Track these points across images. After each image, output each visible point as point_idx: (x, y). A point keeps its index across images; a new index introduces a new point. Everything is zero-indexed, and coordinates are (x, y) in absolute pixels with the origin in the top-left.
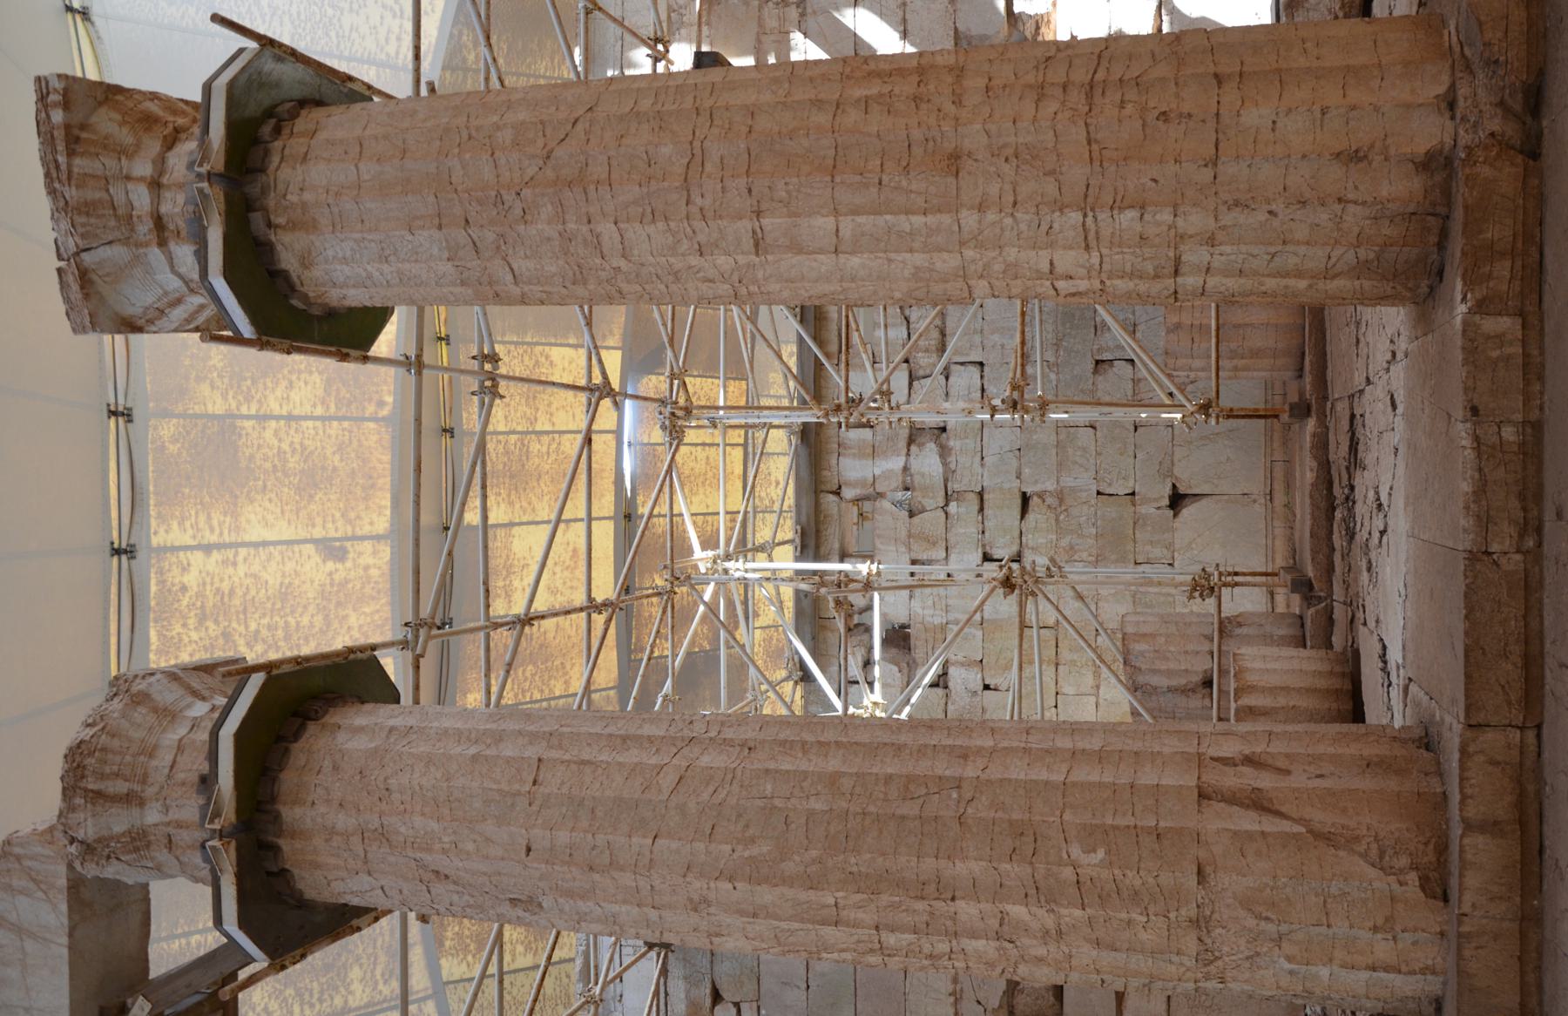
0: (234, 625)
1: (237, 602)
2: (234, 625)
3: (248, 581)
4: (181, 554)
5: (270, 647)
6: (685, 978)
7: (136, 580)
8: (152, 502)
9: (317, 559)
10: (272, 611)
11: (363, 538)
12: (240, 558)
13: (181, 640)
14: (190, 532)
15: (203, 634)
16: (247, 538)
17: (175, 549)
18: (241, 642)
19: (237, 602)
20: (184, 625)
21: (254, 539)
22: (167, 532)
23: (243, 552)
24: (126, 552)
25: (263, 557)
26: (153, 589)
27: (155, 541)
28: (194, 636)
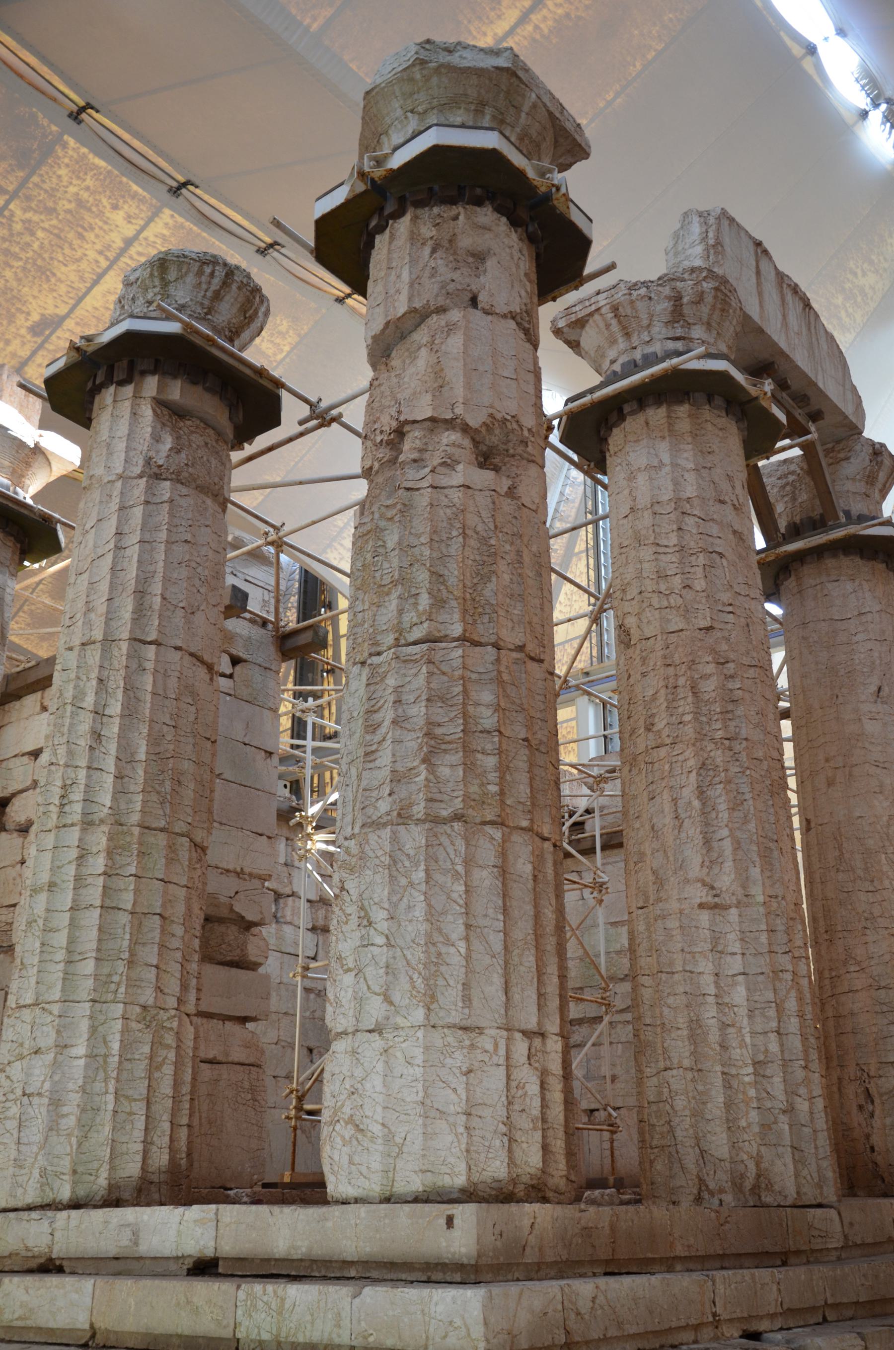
0: (54, 222)
1: (71, 235)
2: (54, 222)
3: (79, 253)
4: (142, 223)
5: (12, 235)
6: (250, 638)
7: (153, 181)
8: (195, 228)
9: (50, 310)
10: (40, 255)
11: (34, 353)
12: (101, 259)
13: (78, 178)
14: (152, 239)
15: (68, 196)
16: (112, 273)
17: (149, 221)
18: (36, 218)
19: (71, 235)
20: (87, 188)
21: (107, 278)
22: (166, 224)
23: (104, 264)
24: (179, 188)
25: (87, 275)
26: (135, 187)
27: (167, 212)
28: (72, 189)
